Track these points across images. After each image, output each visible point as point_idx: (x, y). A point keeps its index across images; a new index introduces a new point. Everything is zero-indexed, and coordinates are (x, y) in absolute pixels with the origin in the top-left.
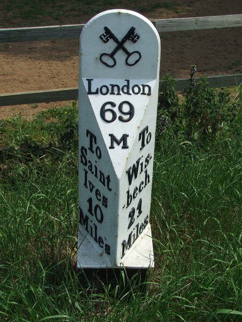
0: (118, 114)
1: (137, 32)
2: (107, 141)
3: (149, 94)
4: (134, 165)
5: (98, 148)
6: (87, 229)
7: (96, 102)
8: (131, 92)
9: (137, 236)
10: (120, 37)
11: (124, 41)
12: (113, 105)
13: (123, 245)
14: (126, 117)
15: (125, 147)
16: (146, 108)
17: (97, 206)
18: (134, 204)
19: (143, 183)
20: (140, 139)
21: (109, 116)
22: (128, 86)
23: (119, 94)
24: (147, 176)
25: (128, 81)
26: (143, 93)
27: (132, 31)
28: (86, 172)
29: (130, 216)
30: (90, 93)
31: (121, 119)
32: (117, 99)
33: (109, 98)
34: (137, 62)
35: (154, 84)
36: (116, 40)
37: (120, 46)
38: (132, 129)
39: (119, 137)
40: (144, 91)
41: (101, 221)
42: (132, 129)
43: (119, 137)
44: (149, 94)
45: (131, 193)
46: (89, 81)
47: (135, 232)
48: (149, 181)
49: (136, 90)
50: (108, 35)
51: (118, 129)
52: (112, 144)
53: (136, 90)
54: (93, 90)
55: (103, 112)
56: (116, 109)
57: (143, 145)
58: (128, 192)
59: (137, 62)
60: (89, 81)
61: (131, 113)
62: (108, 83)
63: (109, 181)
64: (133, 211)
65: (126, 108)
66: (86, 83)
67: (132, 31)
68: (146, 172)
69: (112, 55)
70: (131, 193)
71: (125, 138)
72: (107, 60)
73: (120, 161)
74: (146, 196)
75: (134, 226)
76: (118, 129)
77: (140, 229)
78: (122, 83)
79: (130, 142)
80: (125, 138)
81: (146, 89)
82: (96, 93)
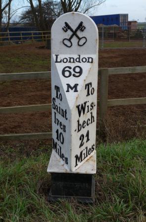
0: (73, 73)
1: (83, 25)
2: (65, 88)
3: (92, 62)
4: (82, 105)
5: (60, 94)
6: (56, 151)
7: (60, 67)
8: (81, 61)
9: (87, 156)
10: (74, 28)
11: (76, 30)
12: (70, 68)
13: (77, 157)
14: (78, 74)
15: (76, 91)
16: (90, 73)
17: (61, 133)
18: (84, 131)
19: (89, 119)
20: (86, 88)
21: (67, 74)
22: (79, 58)
23: (74, 62)
24: (92, 117)
25: (80, 56)
26: (88, 62)
27: (81, 24)
28: (55, 113)
29: (80, 139)
30: (57, 62)
31: (74, 75)
32: (73, 65)
33: (68, 64)
34: (84, 43)
35: (95, 57)
36: (72, 30)
37: (74, 33)
38: (81, 81)
39: (72, 85)
40: (89, 60)
41: (62, 143)
42: (81, 81)
43: (72, 85)
44: (92, 62)
45: (81, 123)
46: (57, 56)
47: (85, 152)
48: (94, 121)
49: (84, 60)
50: (67, 27)
51: (72, 81)
52: (68, 89)
53: (84, 60)
54: (59, 60)
55: (64, 71)
56: (71, 70)
57: (88, 94)
58: (78, 121)
59: (84, 43)
60: (57, 56)
61: (81, 72)
62: (68, 56)
63: (66, 113)
64: (83, 136)
65: (78, 70)
66: (55, 57)
67: (81, 24)
68: (91, 113)
69: (69, 40)
70: (81, 123)
71: (76, 86)
72: (67, 43)
73: (72, 100)
74: (92, 129)
75: (83, 147)
76: (72, 81)
77: (89, 151)
78: (76, 57)
79: (79, 88)
80: (76, 86)
81: (90, 60)
82: (61, 62)
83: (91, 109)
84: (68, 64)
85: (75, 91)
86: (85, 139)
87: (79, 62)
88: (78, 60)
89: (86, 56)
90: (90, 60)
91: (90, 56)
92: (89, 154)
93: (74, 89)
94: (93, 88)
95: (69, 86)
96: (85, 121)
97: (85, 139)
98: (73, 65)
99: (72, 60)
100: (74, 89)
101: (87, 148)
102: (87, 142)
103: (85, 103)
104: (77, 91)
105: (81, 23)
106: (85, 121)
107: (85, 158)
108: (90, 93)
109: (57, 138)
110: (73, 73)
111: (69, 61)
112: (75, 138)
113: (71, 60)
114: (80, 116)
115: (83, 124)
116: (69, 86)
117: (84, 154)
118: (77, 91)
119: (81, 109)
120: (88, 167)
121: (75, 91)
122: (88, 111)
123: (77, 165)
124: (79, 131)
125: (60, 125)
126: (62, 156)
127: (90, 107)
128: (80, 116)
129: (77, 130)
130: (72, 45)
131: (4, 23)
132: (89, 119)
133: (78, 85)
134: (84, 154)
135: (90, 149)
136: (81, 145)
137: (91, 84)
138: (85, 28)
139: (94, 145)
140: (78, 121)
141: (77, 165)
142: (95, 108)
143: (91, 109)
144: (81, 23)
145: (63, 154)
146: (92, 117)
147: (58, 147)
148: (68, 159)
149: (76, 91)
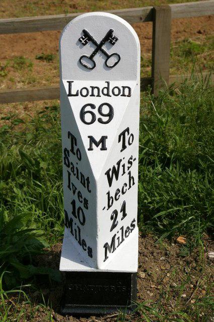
0: (98, 116)
1: (114, 35)
2: (86, 143)
3: (129, 96)
4: (114, 168)
5: (78, 150)
7: (76, 104)
8: (111, 93)
9: (123, 240)
10: (98, 43)
11: (102, 43)
12: (93, 106)
13: (106, 246)
14: (105, 119)
15: (104, 148)
16: (128, 112)
17: (80, 208)
18: (117, 206)
19: (126, 185)
20: (119, 141)
21: (88, 118)
22: (108, 88)
23: (99, 96)
24: (131, 178)
25: (108, 83)
26: (124, 95)
27: (110, 33)
28: (69, 174)
29: (112, 218)
30: (70, 95)
31: (100, 121)
32: (97, 101)
33: (90, 100)
34: (116, 64)
35: (135, 85)
36: (94, 43)
37: (99, 48)
38: (112, 131)
39: (98, 139)
40: (124, 92)
41: (83, 224)
42: (112, 131)
43: (98, 139)
44: (129, 96)
45: (112, 194)
46: (70, 83)
47: (120, 235)
48: (134, 184)
49: (116, 91)
50: (87, 37)
51: (97, 130)
52: (91, 145)
53: (116, 91)
54: (74, 92)
55: (82, 114)
56: (95, 111)
57: (124, 147)
58: (108, 193)
59: (116, 64)
60: (70, 83)
61: (110, 115)
62: (88, 84)
63: (88, 182)
64: (116, 212)
65: (106, 110)
66: (66, 86)
67: (110, 33)
68: (130, 173)
69: (91, 58)
70: (112, 194)
71: (104, 139)
72: (87, 64)
73: (99, 162)
74: (131, 199)
75: (118, 228)
76: (97, 130)
77: (126, 232)
78: (102, 85)
79: (108, 143)
80: (104, 139)
81: (127, 92)
82: (77, 95)
83: (129, 168)
84: (90, 100)
85: (101, 149)
86: (120, 215)
87: (108, 95)
88: (105, 91)
89: (120, 84)
90: (127, 92)
91: (126, 84)
92: (126, 237)
93: (100, 146)
94: (132, 135)
95: (92, 139)
96: (118, 190)
97: (120, 215)
98: (97, 101)
99: (96, 91)
100: (100, 146)
101: (122, 228)
102: (122, 219)
103: (118, 164)
104: (106, 149)
105: (111, 32)
106: (118, 190)
107: (119, 245)
108: (127, 144)
109: (74, 213)
110: (98, 116)
111: (90, 93)
112: (103, 218)
113: (93, 91)
114: (110, 185)
115: (116, 195)
116: (92, 139)
117: (118, 238)
118: (106, 149)
119: (112, 174)
120: (124, 258)
121: (101, 149)
122: (124, 173)
123: (106, 257)
124: (109, 206)
125: (79, 196)
126: (83, 243)
127: (127, 165)
128: (110, 185)
129: (107, 207)
130: (95, 66)
131: (7, 222)
132: (126, 185)
133: (106, 137)
134: (118, 238)
135: (128, 228)
136: (114, 226)
137: (128, 130)
138: (117, 40)
139: (134, 221)
140: (108, 193)
141: (106, 257)
142: (136, 164)
143: (129, 168)
144: (111, 32)
145: (83, 240)
146: (131, 178)
147: (74, 227)
148: (93, 251)
149: (104, 148)
